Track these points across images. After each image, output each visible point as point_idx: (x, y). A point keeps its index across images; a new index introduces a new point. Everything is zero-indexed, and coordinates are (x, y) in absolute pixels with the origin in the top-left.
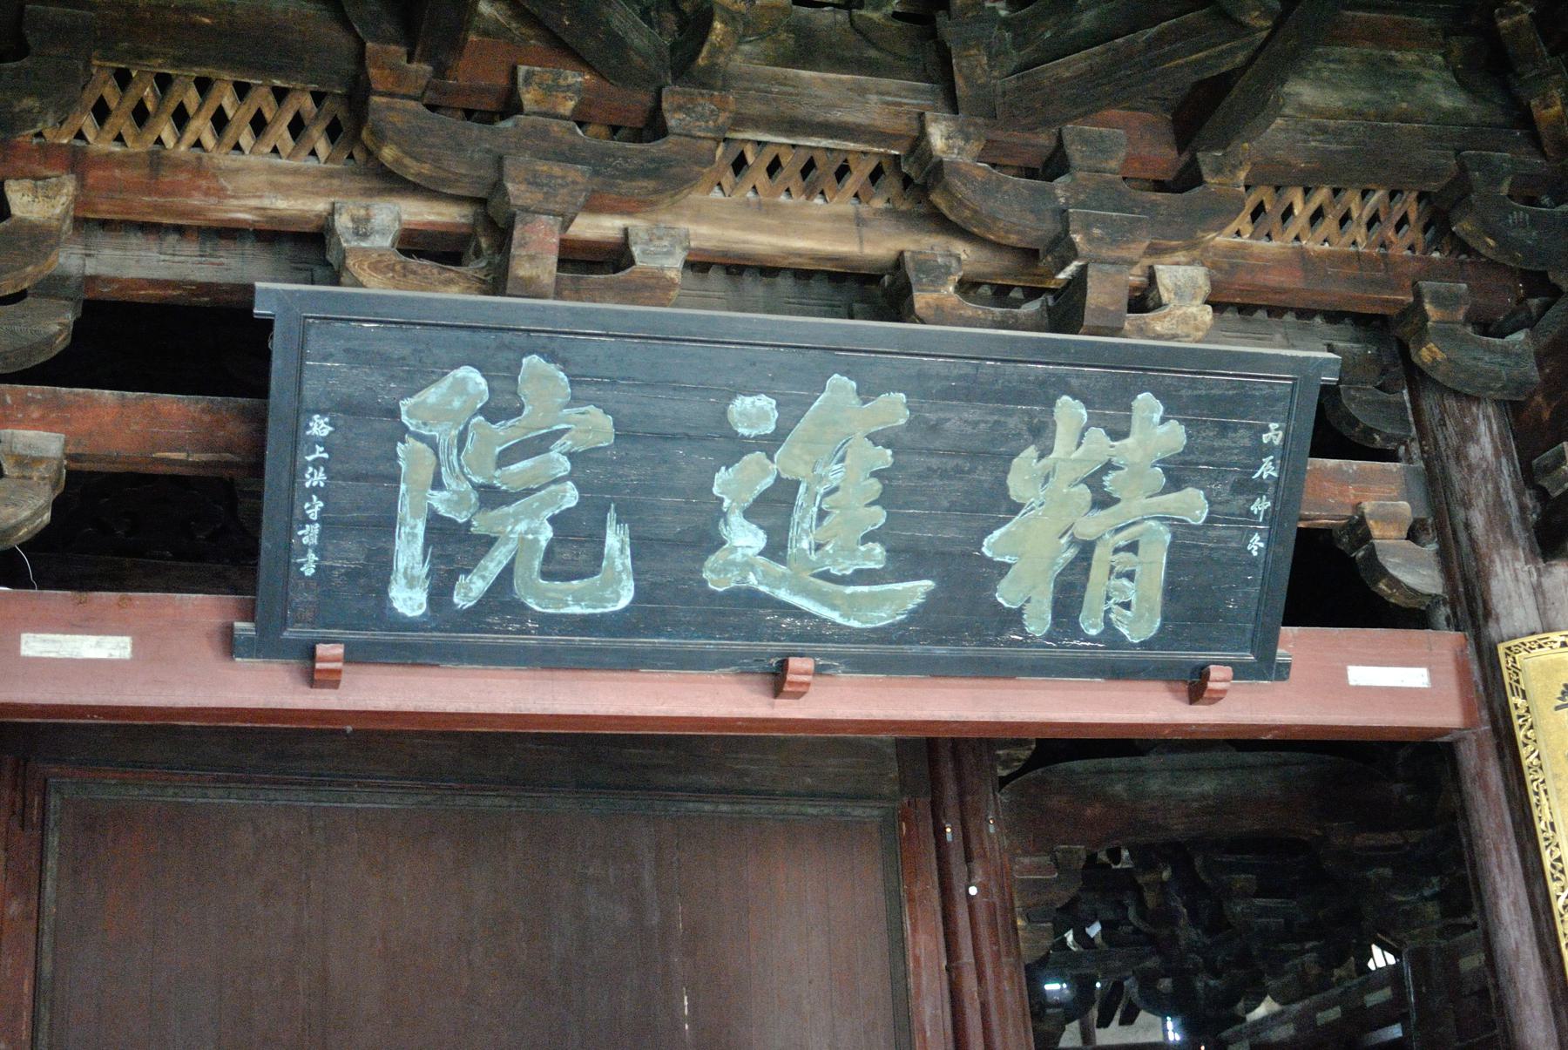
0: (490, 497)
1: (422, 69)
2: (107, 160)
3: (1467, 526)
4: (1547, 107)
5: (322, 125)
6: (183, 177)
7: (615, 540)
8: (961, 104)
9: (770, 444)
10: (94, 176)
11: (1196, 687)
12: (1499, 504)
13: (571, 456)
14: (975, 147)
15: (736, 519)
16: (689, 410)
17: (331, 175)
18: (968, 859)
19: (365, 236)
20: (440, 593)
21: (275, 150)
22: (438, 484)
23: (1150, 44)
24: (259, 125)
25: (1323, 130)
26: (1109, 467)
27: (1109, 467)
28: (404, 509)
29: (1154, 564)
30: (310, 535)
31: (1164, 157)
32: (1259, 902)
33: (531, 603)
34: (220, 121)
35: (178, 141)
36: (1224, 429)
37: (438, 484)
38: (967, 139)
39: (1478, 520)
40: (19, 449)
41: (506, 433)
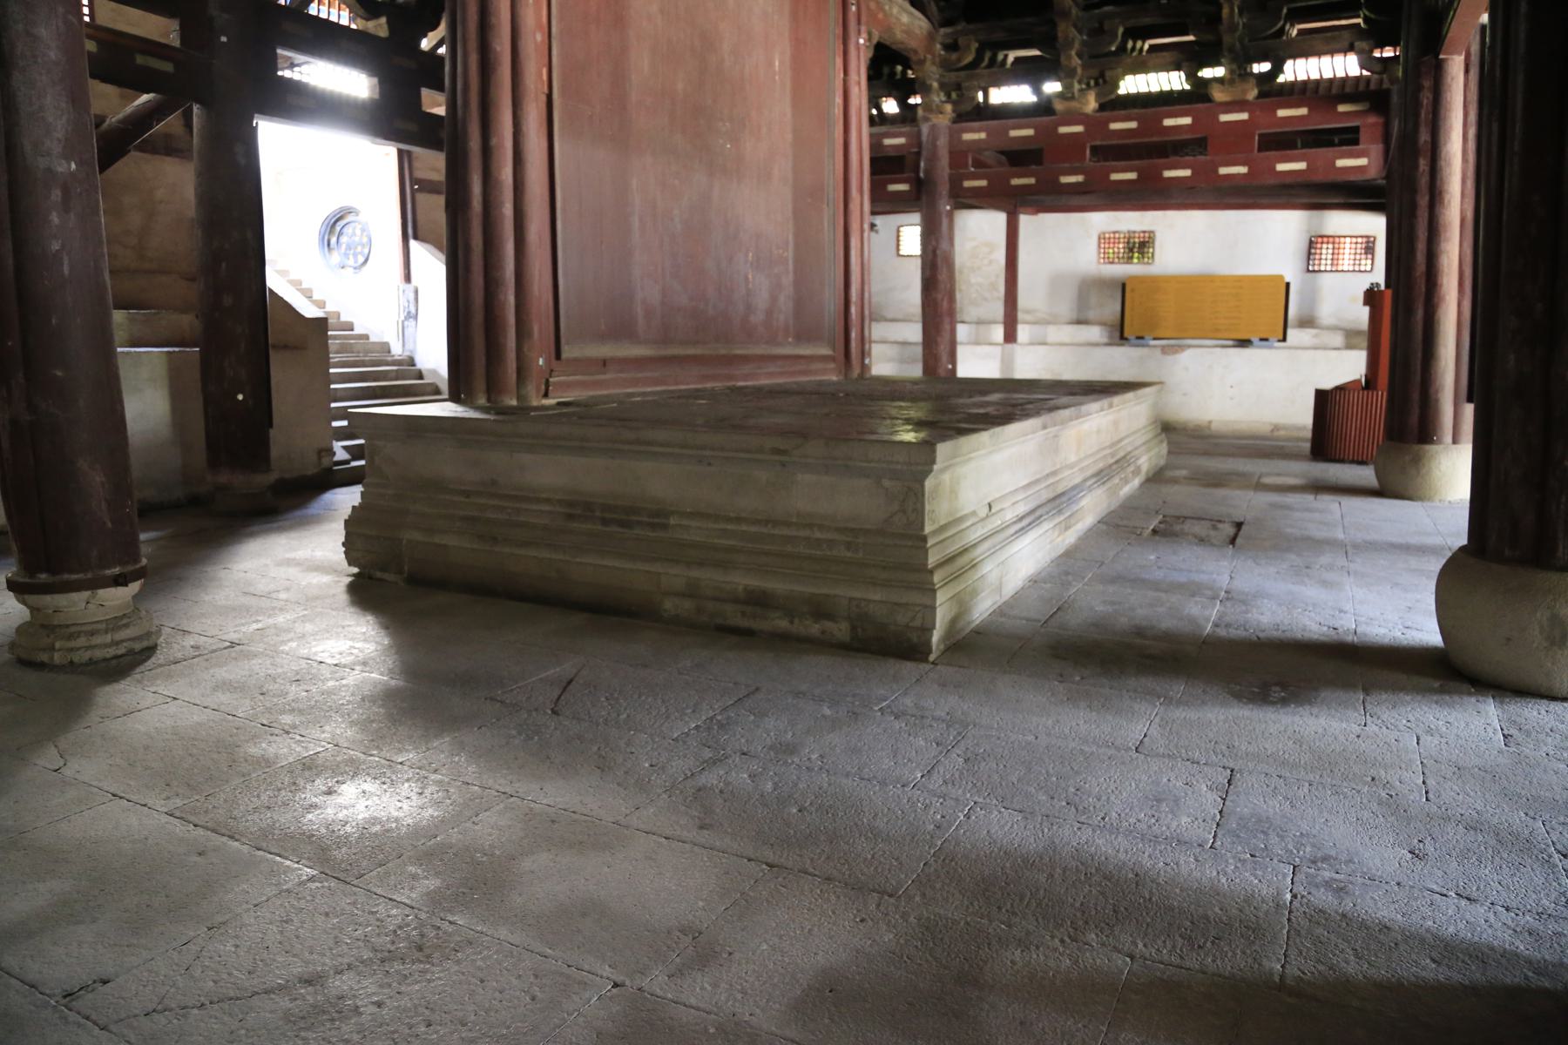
18: (859, 23)
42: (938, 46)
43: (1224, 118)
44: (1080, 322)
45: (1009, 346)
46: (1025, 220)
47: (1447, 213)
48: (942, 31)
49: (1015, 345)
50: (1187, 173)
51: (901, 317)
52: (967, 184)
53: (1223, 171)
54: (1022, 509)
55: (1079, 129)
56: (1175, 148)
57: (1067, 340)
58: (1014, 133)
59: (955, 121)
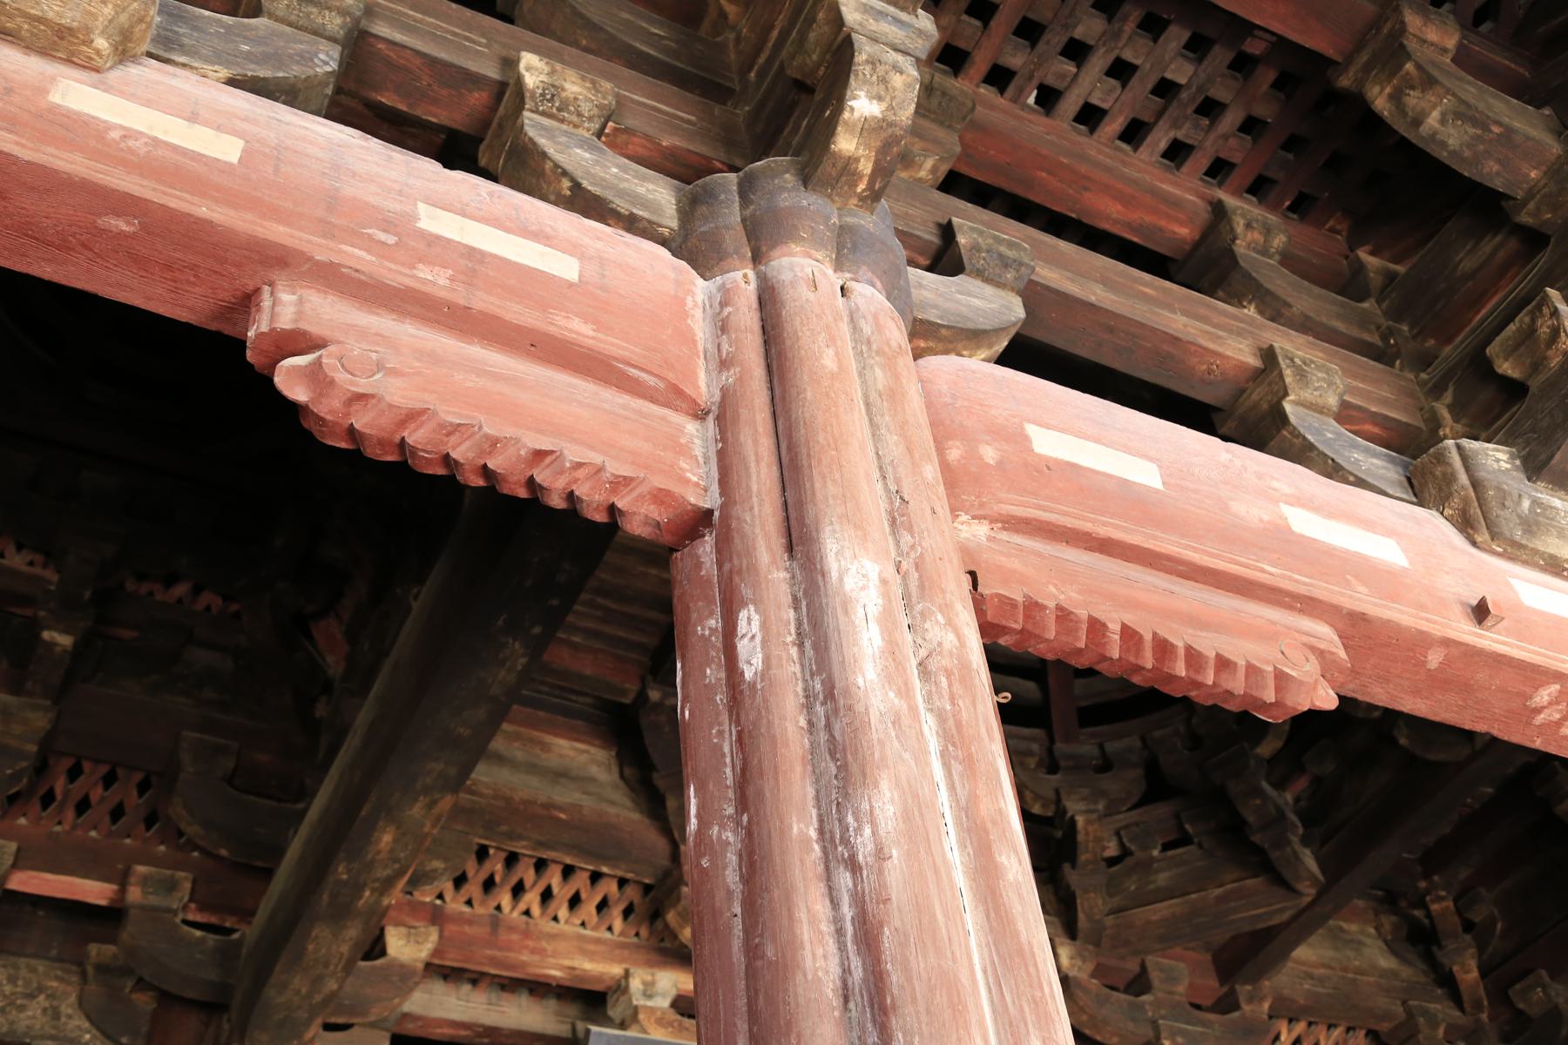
2: (460, 919)
4: (1467, 972)
5: (622, 906)
6: (515, 937)
8: (1080, 935)
10: (451, 928)
14: (1090, 966)
17: (623, 946)
19: (650, 997)
21: (583, 924)
23: (1219, 899)
24: (575, 902)
25: (1311, 977)
31: (1212, 986)
34: (547, 895)
35: (513, 908)
38: (1084, 961)
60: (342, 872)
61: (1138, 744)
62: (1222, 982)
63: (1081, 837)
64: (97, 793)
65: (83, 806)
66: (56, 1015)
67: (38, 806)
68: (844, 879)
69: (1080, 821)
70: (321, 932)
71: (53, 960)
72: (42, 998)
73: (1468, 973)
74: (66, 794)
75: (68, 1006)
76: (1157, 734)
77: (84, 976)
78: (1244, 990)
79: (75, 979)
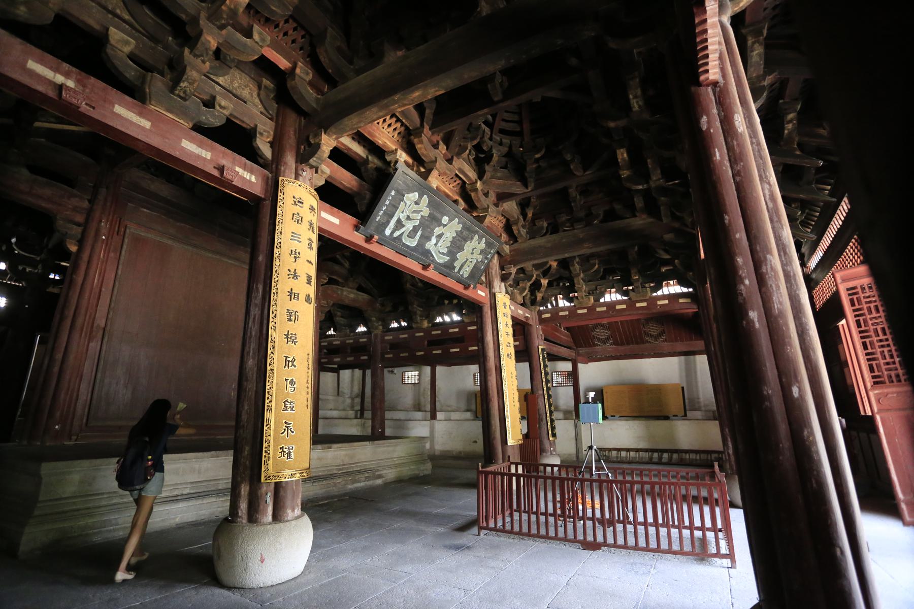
0: (408, 218)
1: (430, 133)
3: (492, 273)
5: (398, 131)
7: (419, 233)
9: (445, 226)
11: (466, 287)
12: (496, 271)
13: (422, 216)
15: (434, 236)
16: (438, 215)
20: (392, 233)
22: (402, 213)
23: (511, 184)
24: (390, 125)
26: (475, 248)
27: (475, 248)
28: (396, 215)
29: (472, 265)
30: (381, 213)
32: (341, 319)
33: (403, 240)
36: (488, 248)
37: (402, 213)
39: (494, 272)
40: (322, 168)
41: (416, 207)
42: (378, 305)
43: (469, 328)
44: (468, 410)
45: (432, 421)
46: (439, 369)
47: (488, 364)
48: (380, 299)
49: (435, 421)
50: (458, 350)
51: (402, 409)
52: (386, 356)
53: (470, 349)
54: (187, 491)
55: (422, 334)
56: (458, 340)
57: (458, 418)
58: (402, 336)
59: (383, 332)
60: (396, 97)
61: (509, 142)
62: (497, 200)
63: (493, 159)
64: (290, 32)
65: (286, 34)
66: (252, 96)
67: (273, 27)
68: (766, 186)
69: (495, 155)
70: (375, 109)
71: (252, 78)
72: (248, 88)
73: (530, 215)
74: (283, 27)
75: (255, 94)
76: (514, 142)
77: (260, 88)
78: (500, 203)
79: (256, 87)
